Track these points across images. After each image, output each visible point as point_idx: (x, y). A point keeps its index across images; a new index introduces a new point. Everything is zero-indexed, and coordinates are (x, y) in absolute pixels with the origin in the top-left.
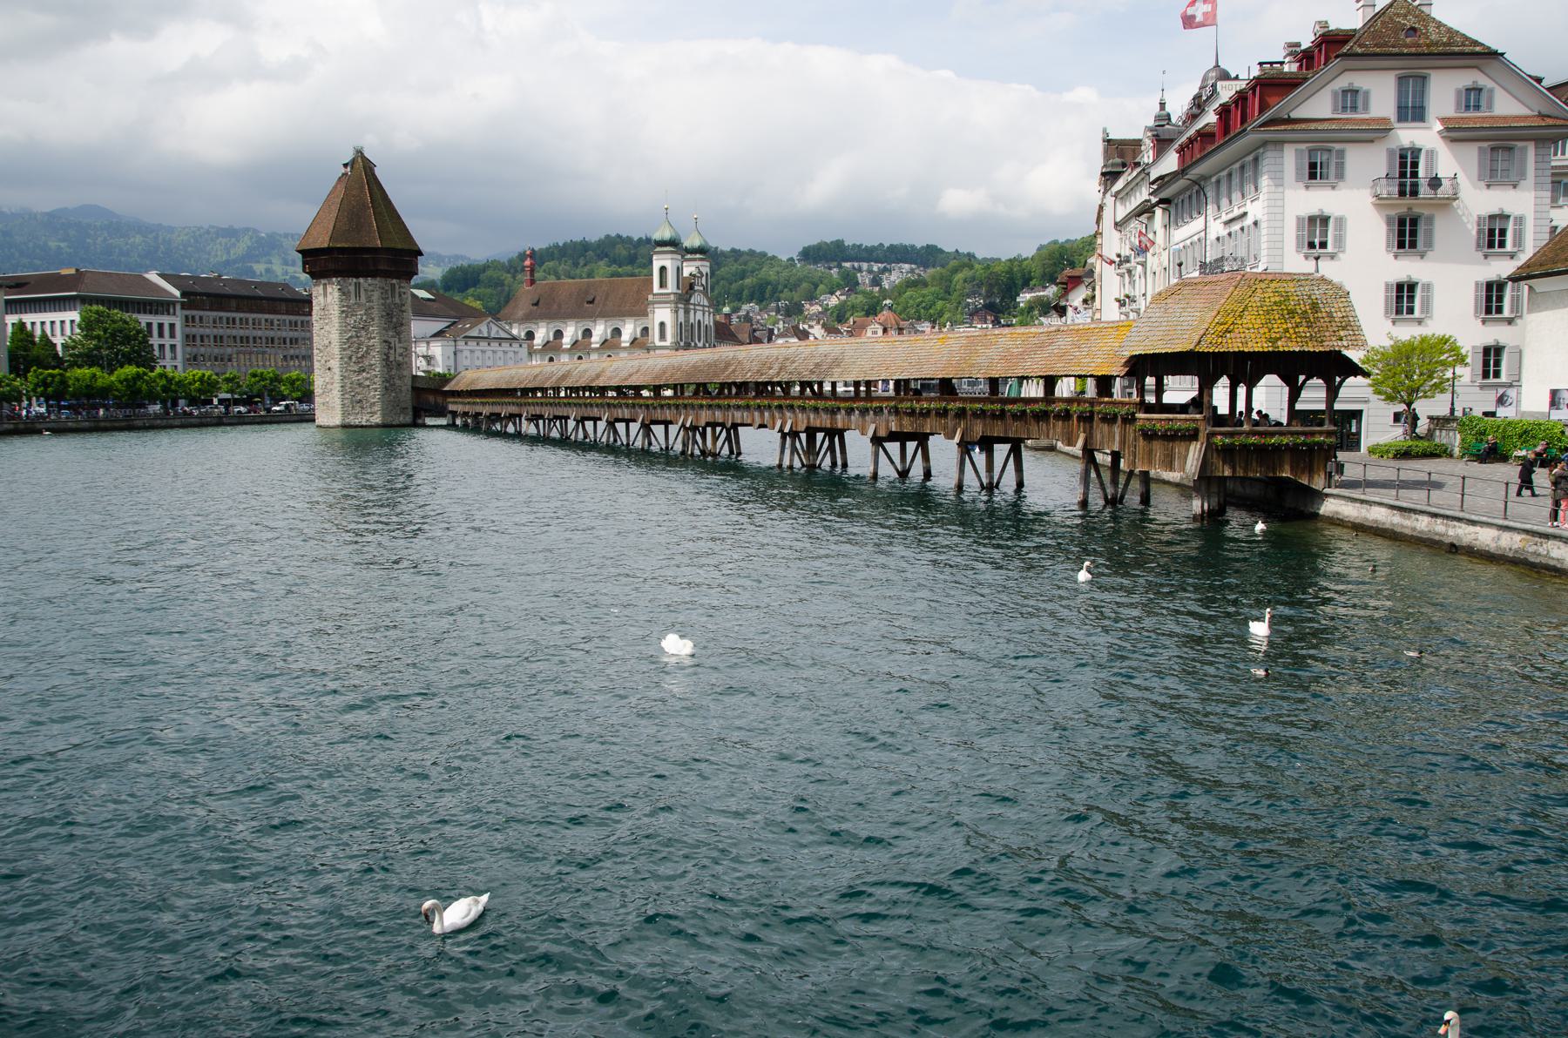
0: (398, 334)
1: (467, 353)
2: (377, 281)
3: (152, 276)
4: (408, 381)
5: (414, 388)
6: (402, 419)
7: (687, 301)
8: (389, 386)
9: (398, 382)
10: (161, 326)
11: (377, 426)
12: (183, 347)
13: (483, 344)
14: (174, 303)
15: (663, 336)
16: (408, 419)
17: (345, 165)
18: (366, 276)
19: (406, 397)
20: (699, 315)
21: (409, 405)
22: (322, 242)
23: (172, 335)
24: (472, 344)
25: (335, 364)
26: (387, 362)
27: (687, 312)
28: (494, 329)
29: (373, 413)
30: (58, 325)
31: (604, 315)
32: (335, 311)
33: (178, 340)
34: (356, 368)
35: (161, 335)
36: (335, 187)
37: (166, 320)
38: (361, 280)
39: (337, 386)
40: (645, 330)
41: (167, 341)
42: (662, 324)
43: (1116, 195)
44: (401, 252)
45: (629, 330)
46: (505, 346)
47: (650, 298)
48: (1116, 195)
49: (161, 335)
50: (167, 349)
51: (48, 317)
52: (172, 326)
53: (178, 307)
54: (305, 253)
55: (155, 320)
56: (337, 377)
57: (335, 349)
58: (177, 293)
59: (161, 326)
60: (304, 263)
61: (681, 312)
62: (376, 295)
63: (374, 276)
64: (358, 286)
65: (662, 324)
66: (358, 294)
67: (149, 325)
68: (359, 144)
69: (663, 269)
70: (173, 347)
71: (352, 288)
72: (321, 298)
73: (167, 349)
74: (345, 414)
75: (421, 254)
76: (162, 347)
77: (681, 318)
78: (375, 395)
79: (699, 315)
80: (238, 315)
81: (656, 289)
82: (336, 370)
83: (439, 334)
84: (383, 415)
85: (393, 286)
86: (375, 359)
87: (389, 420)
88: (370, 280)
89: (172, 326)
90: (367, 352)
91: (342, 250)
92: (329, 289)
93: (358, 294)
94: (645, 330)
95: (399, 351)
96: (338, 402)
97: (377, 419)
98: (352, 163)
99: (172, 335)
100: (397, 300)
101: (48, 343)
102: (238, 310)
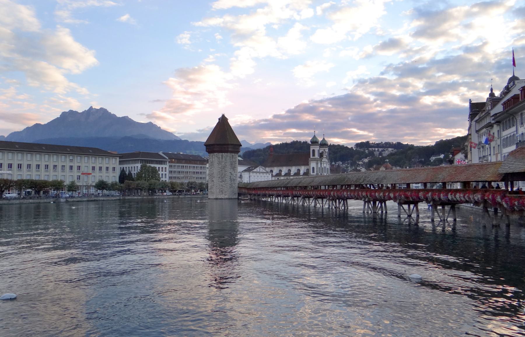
1: (253, 177)
2: (229, 154)
3: (161, 153)
7: (321, 161)
10: (162, 168)
11: (227, 199)
13: (258, 174)
15: (313, 172)
16: (236, 197)
18: (225, 152)
20: (325, 165)
21: (237, 192)
22: (212, 142)
23: (165, 171)
24: (255, 174)
27: (321, 164)
28: (261, 169)
30: (133, 168)
31: (295, 165)
33: (167, 173)
35: (162, 171)
37: (164, 166)
40: (308, 170)
41: (164, 173)
42: (313, 168)
43: (476, 121)
45: (303, 169)
46: (265, 174)
47: (310, 159)
48: (476, 121)
49: (162, 171)
50: (164, 175)
51: (130, 166)
52: (166, 168)
55: (161, 166)
59: (162, 168)
60: (206, 149)
61: (319, 164)
62: (228, 158)
63: (227, 152)
64: (222, 156)
65: (313, 168)
66: (222, 158)
67: (159, 168)
69: (314, 151)
70: (165, 174)
71: (221, 156)
73: (164, 175)
76: (162, 174)
77: (319, 165)
79: (325, 165)
80: (185, 165)
81: (311, 157)
83: (245, 171)
87: (230, 197)
88: (226, 154)
89: (166, 168)
93: (222, 158)
94: (308, 170)
97: (226, 197)
99: (165, 171)
101: (130, 174)
102: (185, 163)
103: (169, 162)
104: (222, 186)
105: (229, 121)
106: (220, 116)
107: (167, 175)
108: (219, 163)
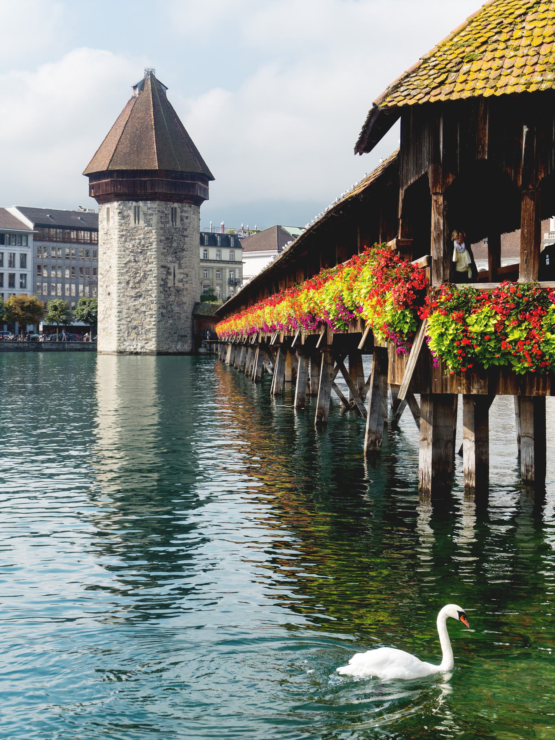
0: (179, 259)
4: (188, 308)
5: (195, 316)
6: (179, 347)
8: (165, 312)
9: (176, 309)
12: (34, 276)
14: (26, 235)
16: (187, 347)
17: (135, 87)
18: (145, 199)
19: (185, 324)
21: (189, 332)
22: (102, 166)
25: (114, 289)
26: (163, 286)
29: (147, 340)
32: (115, 235)
33: (29, 270)
34: (133, 293)
36: (124, 111)
37: (18, 250)
38: (141, 204)
39: (114, 312)
41: (17, 271)
44: (182, 175)
52: (24, 257)
53: (31, 238)
54: (93, 176)
56: (115, 303)
57: (114, 275)
58: (30, 225)
60: (91, 187)
62: (155, 219)
63: (152, 198)
68: (149, 65)
70: (23, 276)
72: (105, 222)
74: (121, 340)
75: (213, 179)
78: (150, 322)
82: (114, 295)
84: (158, 342)
85: (174, 210)
86: (152, 284)
87: (165, 348)
90: (145, 277)
91: (121, 173)
92: (111, 214)
95: (178, 277)
96: (115, 327)
98: (141, 86)
99: (23, 265)
100: (178, 224)
103: (36, 238)
104: (136, 310)
105: (170, 96)
106: (140, 77)
107: (29, 278)
108: (126, 235)
